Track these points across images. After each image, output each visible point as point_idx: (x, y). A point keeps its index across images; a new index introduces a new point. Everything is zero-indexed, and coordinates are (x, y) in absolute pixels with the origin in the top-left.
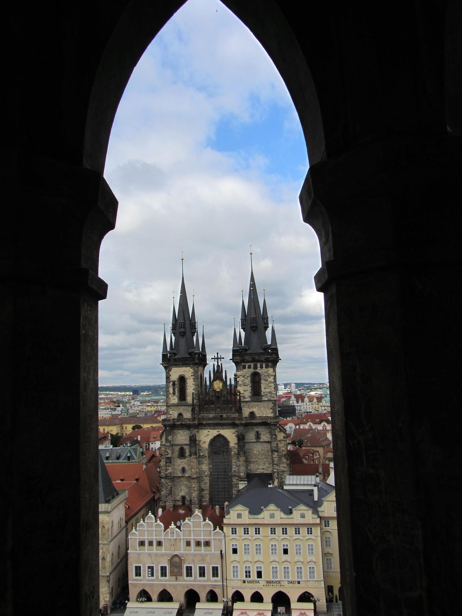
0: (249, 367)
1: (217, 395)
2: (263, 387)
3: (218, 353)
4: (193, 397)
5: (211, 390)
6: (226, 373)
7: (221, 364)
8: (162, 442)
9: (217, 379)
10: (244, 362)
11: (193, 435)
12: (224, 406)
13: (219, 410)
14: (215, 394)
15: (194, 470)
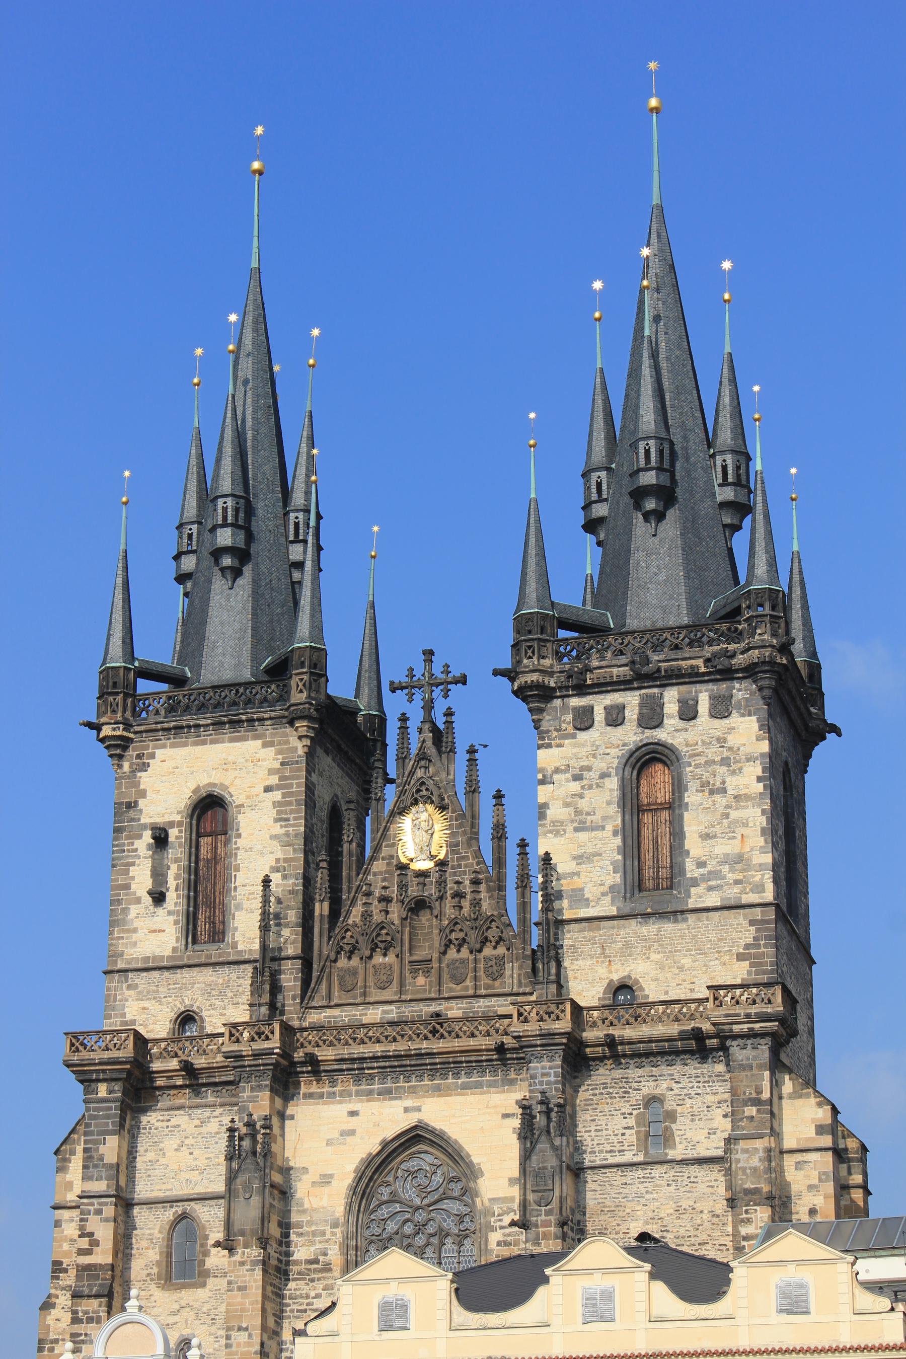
0: (615, 718)
1: (413, 891)
2: (693, 824)
3: (429, 654)
4: (266, 902)
5: (378, 866)
6: (472, 762)
7: (449, 713)
8: (69, 1186)
9: (416, 802)
10: (582, 689)
11: (250, 1124)
12: (452, 953)
13: (421, 980)
14: (403, 887)
15: (242, 1337)
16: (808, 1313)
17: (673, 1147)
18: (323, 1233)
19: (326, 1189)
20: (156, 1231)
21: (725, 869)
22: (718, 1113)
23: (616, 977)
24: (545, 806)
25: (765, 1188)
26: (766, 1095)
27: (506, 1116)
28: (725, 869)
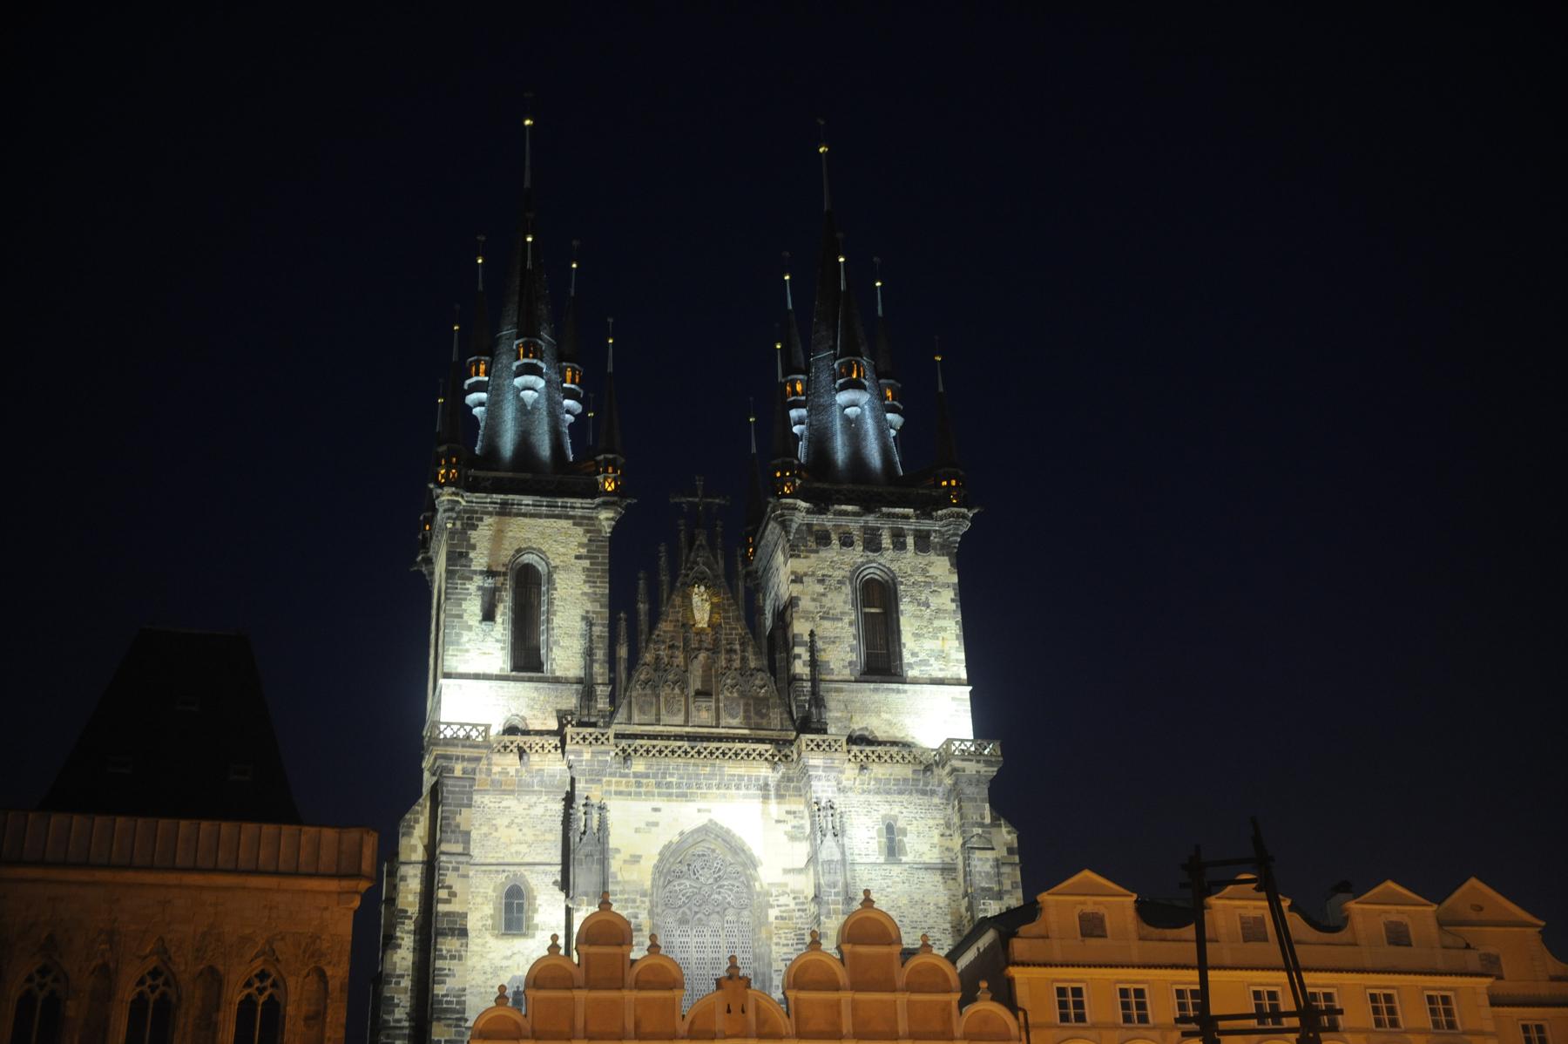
0: (847, 542)
2: (907, 627)
8: (414, 849)
16: (1410, 945)
17: (905, 854)
18: (634, 901)
19: (636, 867)
20: (490, 892)
21: (932, 661)
22: (936, 833)
23: (856, 727)
24: (797, 598)
25: (996, 888)
26: (988, 820)
27: (778, 821)
28: (932, 661)
